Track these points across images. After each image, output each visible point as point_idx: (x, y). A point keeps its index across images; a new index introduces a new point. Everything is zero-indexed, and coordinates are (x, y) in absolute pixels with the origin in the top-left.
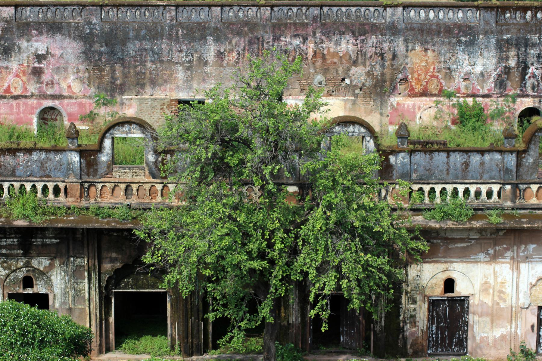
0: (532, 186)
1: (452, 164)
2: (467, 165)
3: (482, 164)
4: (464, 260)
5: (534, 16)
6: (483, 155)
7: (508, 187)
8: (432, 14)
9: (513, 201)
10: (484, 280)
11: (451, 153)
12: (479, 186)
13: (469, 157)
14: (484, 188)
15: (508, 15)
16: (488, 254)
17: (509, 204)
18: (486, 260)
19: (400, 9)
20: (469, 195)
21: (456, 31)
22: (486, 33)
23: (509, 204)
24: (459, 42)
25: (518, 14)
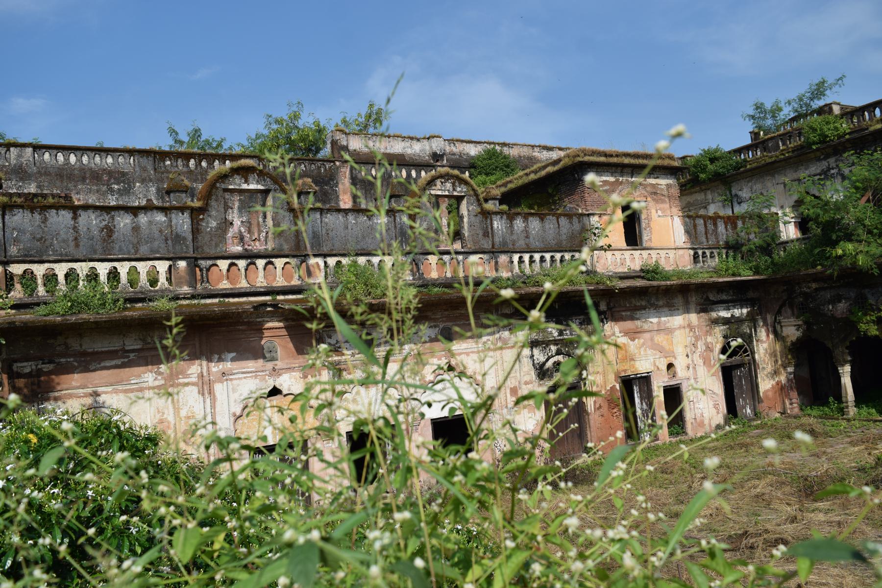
0: (219, 262)
1: (82, 229)
2: (109, 230)
3: (136, 229)
4: (120, 387)
5: (199, 164)
6: (136, 215)
7: (182, 264)
8: (73, 159)
9: (192, 284)
10: (158, 417)
11: (80, 212)
12: (133, 263)
13: (113, 218)
14: (143, 267)
15: (168, 163)
16: (160, 374)
17: (186, 289)
18: (157, 383)
19: (29, 150)
20: (118, 281)
21: (105, 178)
22: (143, 181)
23: (186, 289)
24: (112, 191)
25: (180, 162)
